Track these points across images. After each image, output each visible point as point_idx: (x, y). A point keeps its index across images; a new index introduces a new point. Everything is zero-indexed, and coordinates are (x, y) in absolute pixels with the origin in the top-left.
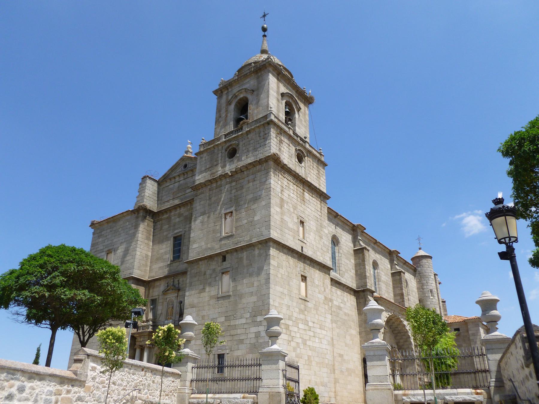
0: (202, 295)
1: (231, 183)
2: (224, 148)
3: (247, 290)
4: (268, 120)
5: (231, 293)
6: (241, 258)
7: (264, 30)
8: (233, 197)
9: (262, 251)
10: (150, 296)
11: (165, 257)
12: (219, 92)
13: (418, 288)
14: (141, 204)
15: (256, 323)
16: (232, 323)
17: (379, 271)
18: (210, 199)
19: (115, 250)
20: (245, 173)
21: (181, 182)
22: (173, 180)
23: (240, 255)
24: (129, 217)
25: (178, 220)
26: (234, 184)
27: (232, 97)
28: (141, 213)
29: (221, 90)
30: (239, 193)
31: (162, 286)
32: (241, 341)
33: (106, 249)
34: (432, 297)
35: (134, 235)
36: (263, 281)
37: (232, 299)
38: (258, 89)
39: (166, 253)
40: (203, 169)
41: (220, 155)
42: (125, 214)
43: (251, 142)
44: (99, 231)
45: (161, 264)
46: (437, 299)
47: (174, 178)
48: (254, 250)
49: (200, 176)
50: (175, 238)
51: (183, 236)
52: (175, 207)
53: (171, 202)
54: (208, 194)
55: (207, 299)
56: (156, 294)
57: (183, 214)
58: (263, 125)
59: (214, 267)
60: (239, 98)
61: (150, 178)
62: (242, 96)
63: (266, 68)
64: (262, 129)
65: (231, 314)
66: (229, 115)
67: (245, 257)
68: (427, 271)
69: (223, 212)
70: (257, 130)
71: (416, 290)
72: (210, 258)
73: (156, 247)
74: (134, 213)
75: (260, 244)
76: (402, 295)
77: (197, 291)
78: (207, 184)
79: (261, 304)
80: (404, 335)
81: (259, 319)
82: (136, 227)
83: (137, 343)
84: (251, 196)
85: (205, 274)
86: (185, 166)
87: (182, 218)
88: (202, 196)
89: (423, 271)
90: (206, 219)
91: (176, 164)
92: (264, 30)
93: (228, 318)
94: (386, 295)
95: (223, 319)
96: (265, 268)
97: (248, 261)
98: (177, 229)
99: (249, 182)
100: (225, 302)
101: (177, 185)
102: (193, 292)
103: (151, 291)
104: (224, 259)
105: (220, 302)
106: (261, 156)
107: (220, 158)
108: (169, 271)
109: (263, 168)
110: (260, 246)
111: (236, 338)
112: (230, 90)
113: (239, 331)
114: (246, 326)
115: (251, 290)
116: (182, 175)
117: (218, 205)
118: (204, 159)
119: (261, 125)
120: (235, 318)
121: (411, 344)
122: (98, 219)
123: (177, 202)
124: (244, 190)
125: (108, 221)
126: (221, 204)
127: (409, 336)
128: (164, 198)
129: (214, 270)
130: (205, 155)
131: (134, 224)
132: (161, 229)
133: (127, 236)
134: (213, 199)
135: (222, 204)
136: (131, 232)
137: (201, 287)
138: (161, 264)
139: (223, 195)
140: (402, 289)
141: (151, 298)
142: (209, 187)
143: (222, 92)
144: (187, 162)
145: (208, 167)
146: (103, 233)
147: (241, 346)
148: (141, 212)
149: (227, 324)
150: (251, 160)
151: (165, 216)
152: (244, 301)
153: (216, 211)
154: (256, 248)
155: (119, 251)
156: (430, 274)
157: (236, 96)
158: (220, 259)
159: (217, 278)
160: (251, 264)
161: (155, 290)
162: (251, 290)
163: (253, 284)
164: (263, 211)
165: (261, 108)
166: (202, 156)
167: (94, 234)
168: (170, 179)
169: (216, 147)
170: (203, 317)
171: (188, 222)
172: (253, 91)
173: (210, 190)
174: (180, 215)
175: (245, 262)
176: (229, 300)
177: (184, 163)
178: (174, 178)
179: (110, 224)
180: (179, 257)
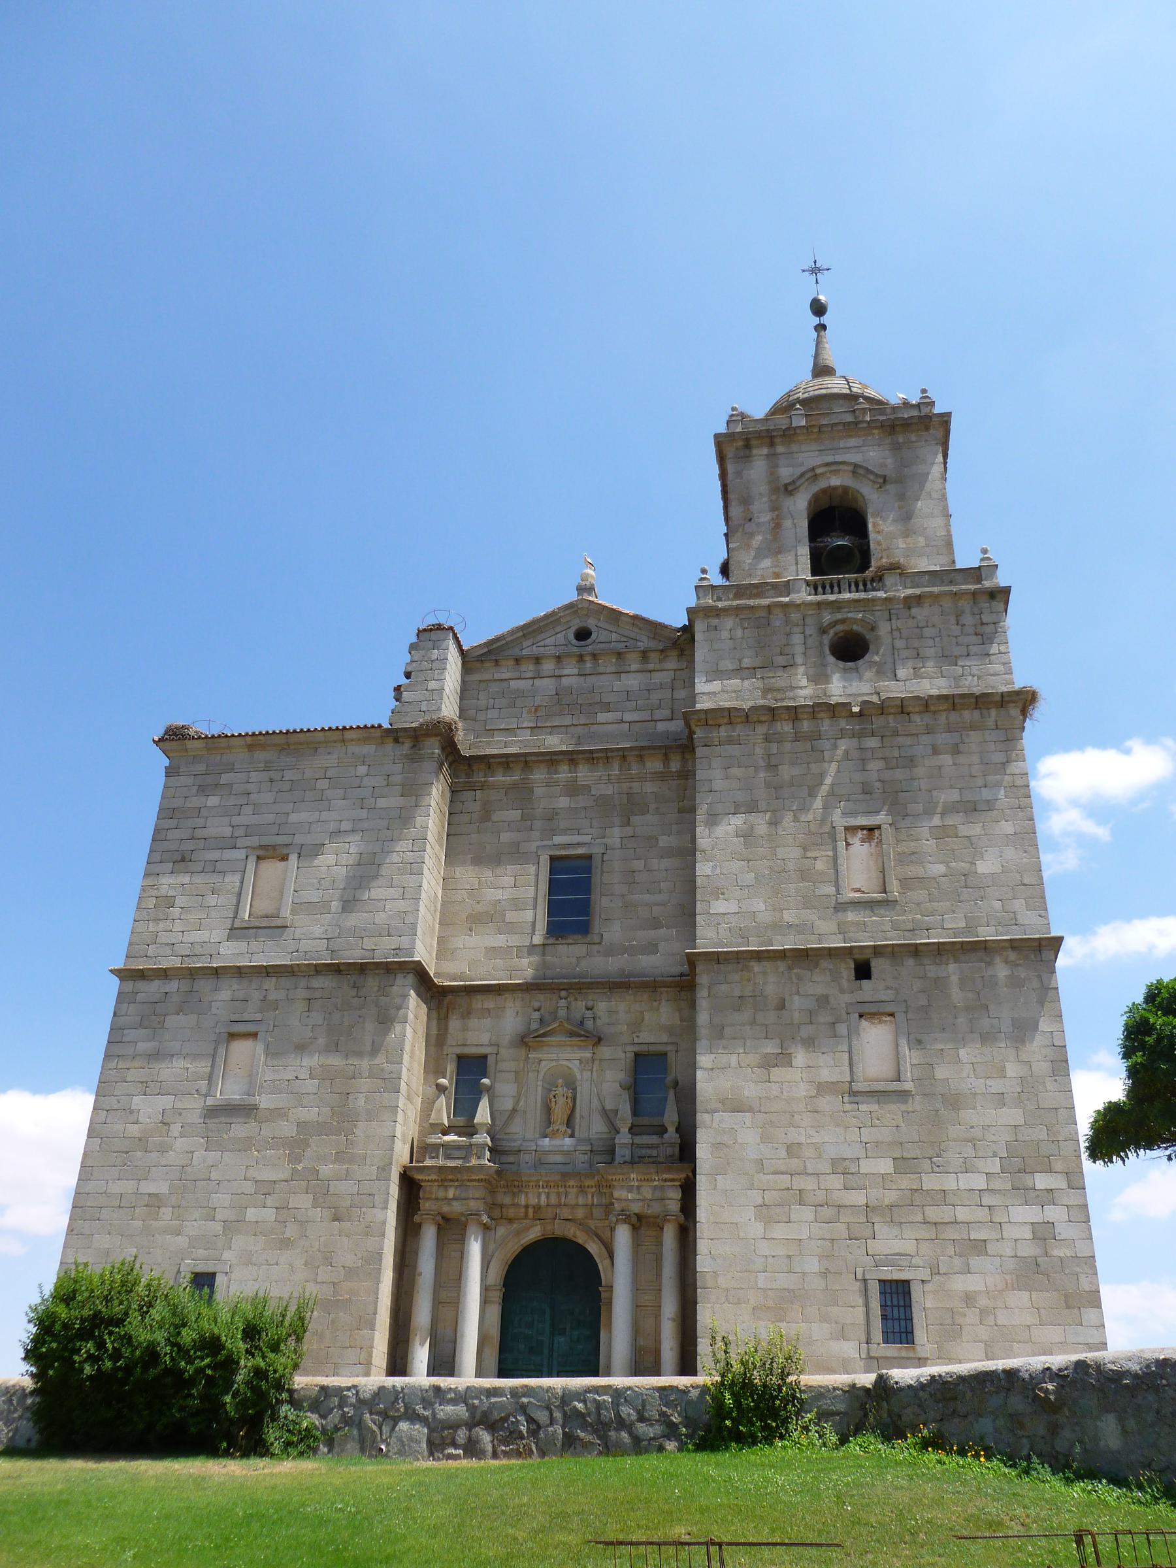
0: (777, 1073)
1: (860, 735)
2: (808, 621)
3: (979, 1085)
4: (987, 584)
5: (908, 1086)
6: (940, 984)
7: (818, 309)
8: (878, 785)
9: (1022, 973)
10: (450, 1040)
11: (510, 916)
12: (738, 445)
14: (435, 717)
15: (1032, 1194)
16: (930, 1182)
18: (772, 767)
19: (309, 852)
20: (916, 718)
21: (565, 681)
22: (528, 668)
23: (932, 970)
24: (369, 749)
25: (564, 802)
26: (872, 742)
27: (802, 475)
28: (433, 748)
29: (747, 440)
30: (900, 774)
31: (511, 1019)
32: (980, 1247)
33: (254, 841)
35: (404, 818)
36: (1041, 1067)
37: (917, 1104)
38: (900, 480)
39: (517, 904)
40: (727, 664)
41: (797, 639)
42: (349, 735)
43: (928, 632)
44: (201, 768)
45: (500, 940)
47: (537, 660)
48: (990, 964)
49: (716, 686)
50: (557, 863)
51: (596, 862)
52: (552, 759)
53: (525, 736)
54: (759, 750)
55: (803, 1090)
56: (485, 1038)
57: (589, 788)
58: (974, 594)
59: (820, 990)
60: (823, 484)
61: (455, 635)
62: (835, 481)
63: (927, 429)
64: (965, 604)
65: (918, 1153)
66: (788, 523)
67: (954, 979)
69: (838, 819)
70: (947, 604)
72: (804, 957)
73: (466, 874)
74: (396, 741)
75: (1013, 948)
77: (752, 1058)
78: (754, 718)
79: (1043, 1135)
81: (1042, 1181)
82: (413, 791)
83: (426, 1205)
84: (954, 795)
85: (782, 1005)
86: (583, 635)
87: (581, 801)
88: (734, 750)
90: (762, 829)
91: (546, 617)
92: (818, 309)
93: (903, 1165)
95: (885, 1166)
96: (1044, 1026)
97: (970, 995)
98: (565, 832)
99: (935, 751)
100: (892, 1112)
101: (547, 686)
102: (734, 1059)
103: (454, 1024)
104: (863, 971)
105: (863, 1107)
106: (972, 685)
107: (799, 649)
108: (544, 965)
109: (990, 722)
110: (1012, 956)
111: (952, 1233)
112: (780, 449)
113: (962, 1214)
114: (987, 1200)
115: (996, 1086)
116: (574, 661)
117: (812, 794)
118: (725, 634)
119: (966, 592)
120: (938, 1169)
122: (208, 720)
123: (554, 742)
124: (920, 771)
125: (256, 741)
126: (824, 789)
128: (492, 713)
129: (823, 1001)
130: (729, 622)
131: (398, 778)
132: (486, 816)
133: (364, 814)
134: (786, 771)
135: (832, 793)
136: (382, 803)
137: (771, 1048)
138: (500, 940)
139: (833, 768)
141: (459, 1051)
142: (761, 729)
143: (748, 446)
144: (591, 623)
145: (747, 662)
146: (225, 778)
147: (976, 1261)
148: (419, 742)
149: (906, 1182)
150: (932, 685)
151: (500, 778)
152: (970, 1116)
153: (803, 809)
154: (997, 960)
155: (325, 860)
157: (815, 477)
158: (847, 970)
159: (842, 1029)
160: (986, 1007)
161: (473, 1023)
162: (996, 1086)
163: (1004, 1069)
164: (1010, 853)
165: (921, 539)
166: (714, 622)
167: (170, 772)
168: (518, 661)
169: (778, 611)
170: (793, 1150)
171: (617, 820)
172: (885, 480)
173: (767, 739)
174: (573, 789)
175: (957, 995)
176: (903, 1107)
177: (576, 624)
178: (537, 660)
179: (261, 755)
180: (584, 929)
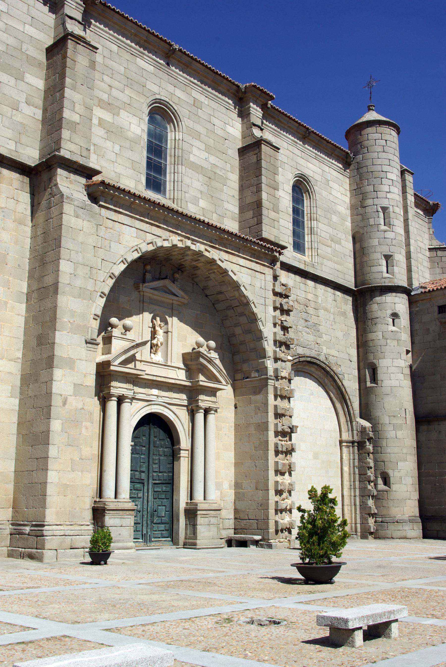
13: (353, 207)
17: (179, 136)
34: (383, 227)
46: (401, 231)
68: (379, 162)
71: (348, 212)
76: (259, 204)
80: (242, 314)
89: (369, 162)
94: (202, 203)
121: (259, 337)
127: (253, 314)
140: (259, 190)
156: (385, 168)
